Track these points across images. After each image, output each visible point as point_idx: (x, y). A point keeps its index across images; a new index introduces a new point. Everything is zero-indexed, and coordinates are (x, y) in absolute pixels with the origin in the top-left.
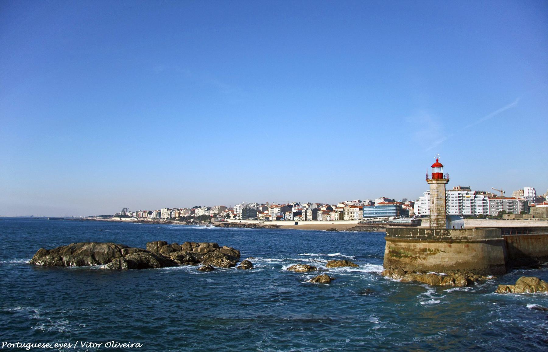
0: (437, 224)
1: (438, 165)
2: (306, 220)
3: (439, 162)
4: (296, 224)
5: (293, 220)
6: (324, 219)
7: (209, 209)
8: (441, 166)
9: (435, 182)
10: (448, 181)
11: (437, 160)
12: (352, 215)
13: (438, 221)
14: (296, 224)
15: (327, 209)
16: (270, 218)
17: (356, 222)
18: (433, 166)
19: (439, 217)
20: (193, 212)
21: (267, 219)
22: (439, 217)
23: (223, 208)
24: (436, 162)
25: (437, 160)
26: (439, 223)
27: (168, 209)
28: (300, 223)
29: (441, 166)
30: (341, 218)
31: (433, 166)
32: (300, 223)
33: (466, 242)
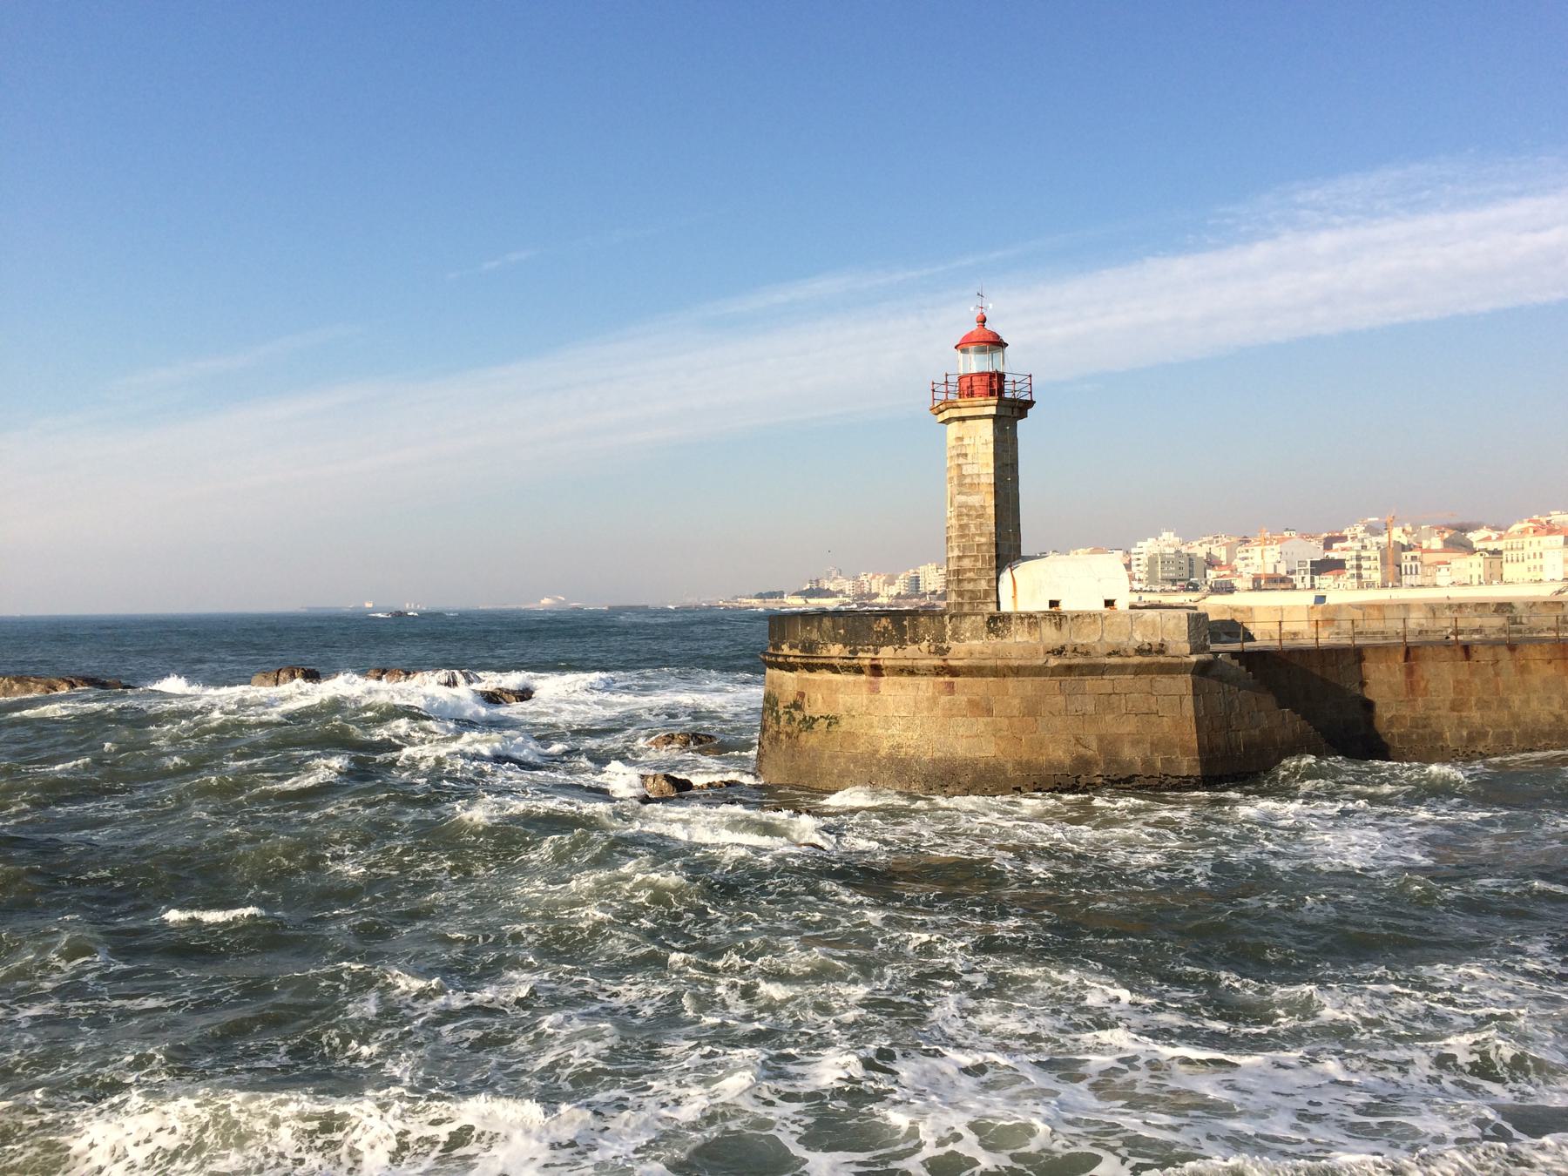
2: (1360, 586)
4: (1320, 599)
5: (1313, 587)
6: (1427, 581)
8: (997, 344)
10: (1030, 403)
12: (1538, 562)
13: (960, 581)
14: (1320, 599)
15: (1446, 542)
16: (1237, 583)
17: (1545, 592)
18: (962, 347)
19: (966, 563)
21: (1230, 589)
22: (966, 563)
24: (974, 326)
26: (970, 586)
28: (1332, 599)
30: (1494, 576)
32: (1332, 599)
33: (939, 671)
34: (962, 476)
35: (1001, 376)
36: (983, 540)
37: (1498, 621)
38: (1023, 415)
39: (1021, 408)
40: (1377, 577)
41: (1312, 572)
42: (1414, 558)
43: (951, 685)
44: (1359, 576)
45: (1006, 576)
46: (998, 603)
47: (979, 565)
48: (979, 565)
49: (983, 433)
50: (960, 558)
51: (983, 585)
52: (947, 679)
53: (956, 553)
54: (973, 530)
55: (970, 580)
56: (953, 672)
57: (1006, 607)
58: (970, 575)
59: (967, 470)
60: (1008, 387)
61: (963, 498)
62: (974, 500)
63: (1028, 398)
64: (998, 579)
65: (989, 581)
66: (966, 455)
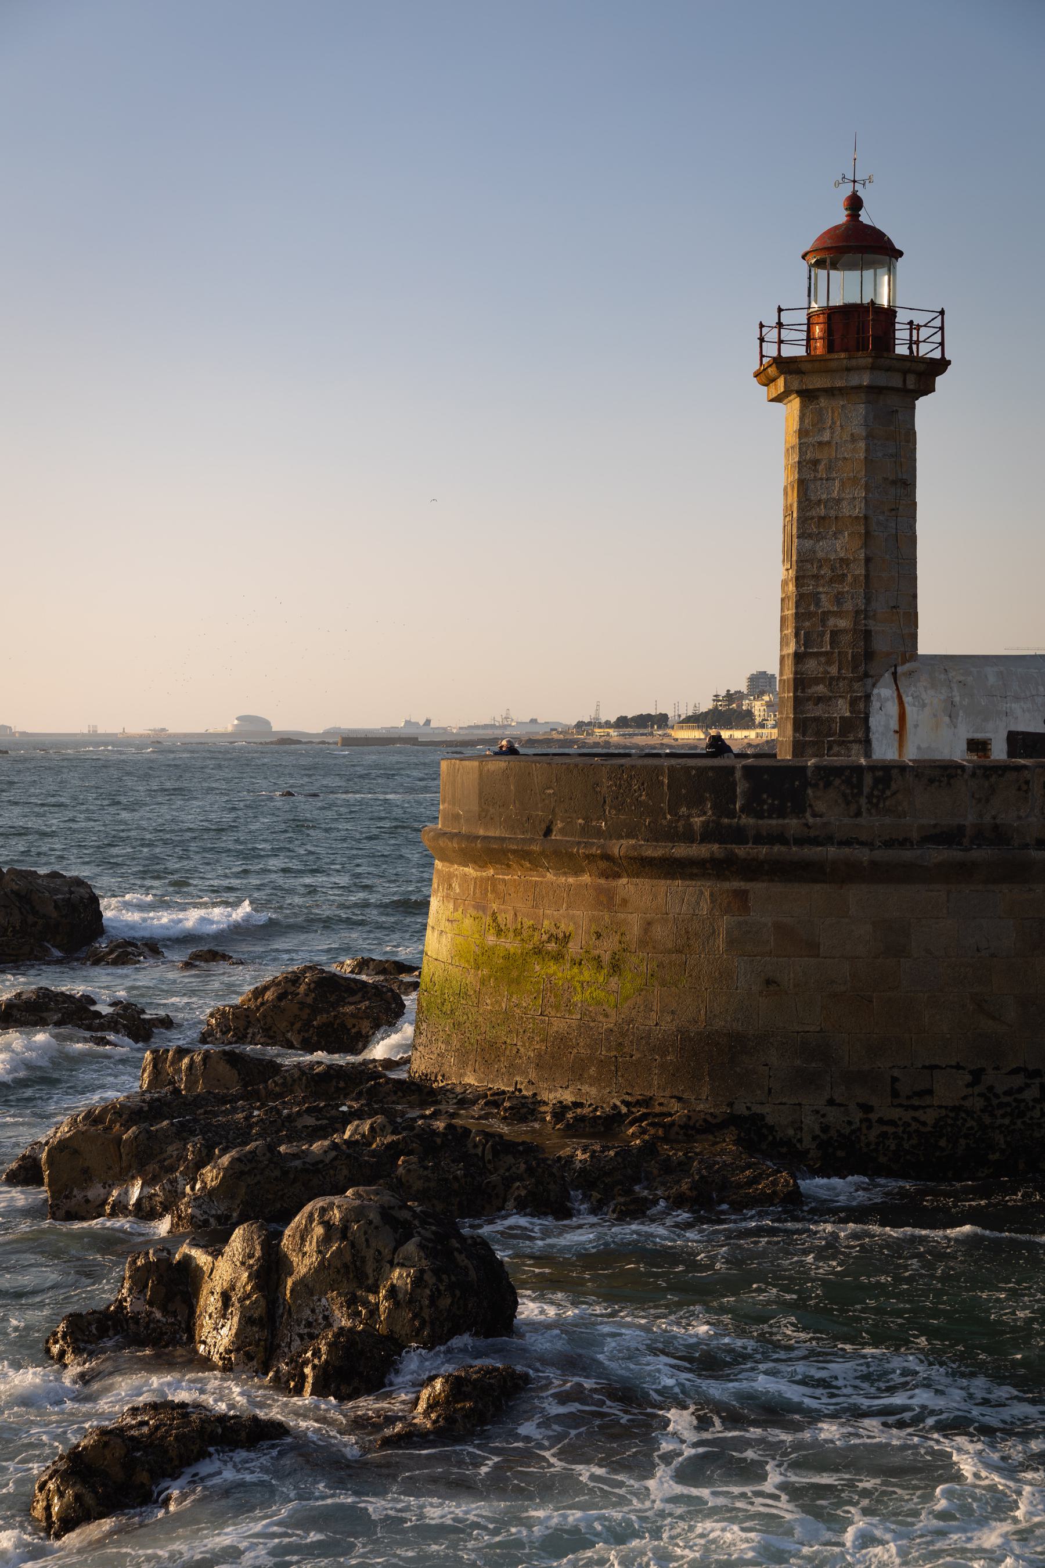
1: (858, 243)
3: (864, 218)
10: (941, 365)
11: (855, 204)
24: (840, 217)
25: (855, 204)
35: (889, 314)
36: (843, 623)
38: (929, 389)
39: (926, 373)
43: (742, 896)
45: (884, 692)
46: (867, 742)
47: (834, 670)
48: (834, 670)
51: (842, 708)
52: (737, 884)
54: (826, 604)
55: (819, 700)
56: (751, 870)
57: (884, 750)
58: (821, 689)
60: (902, 334)
61: (808, 544)
63: (937, 355)
64: (868, 697)
65: (853, 703)
66: (815, 463)
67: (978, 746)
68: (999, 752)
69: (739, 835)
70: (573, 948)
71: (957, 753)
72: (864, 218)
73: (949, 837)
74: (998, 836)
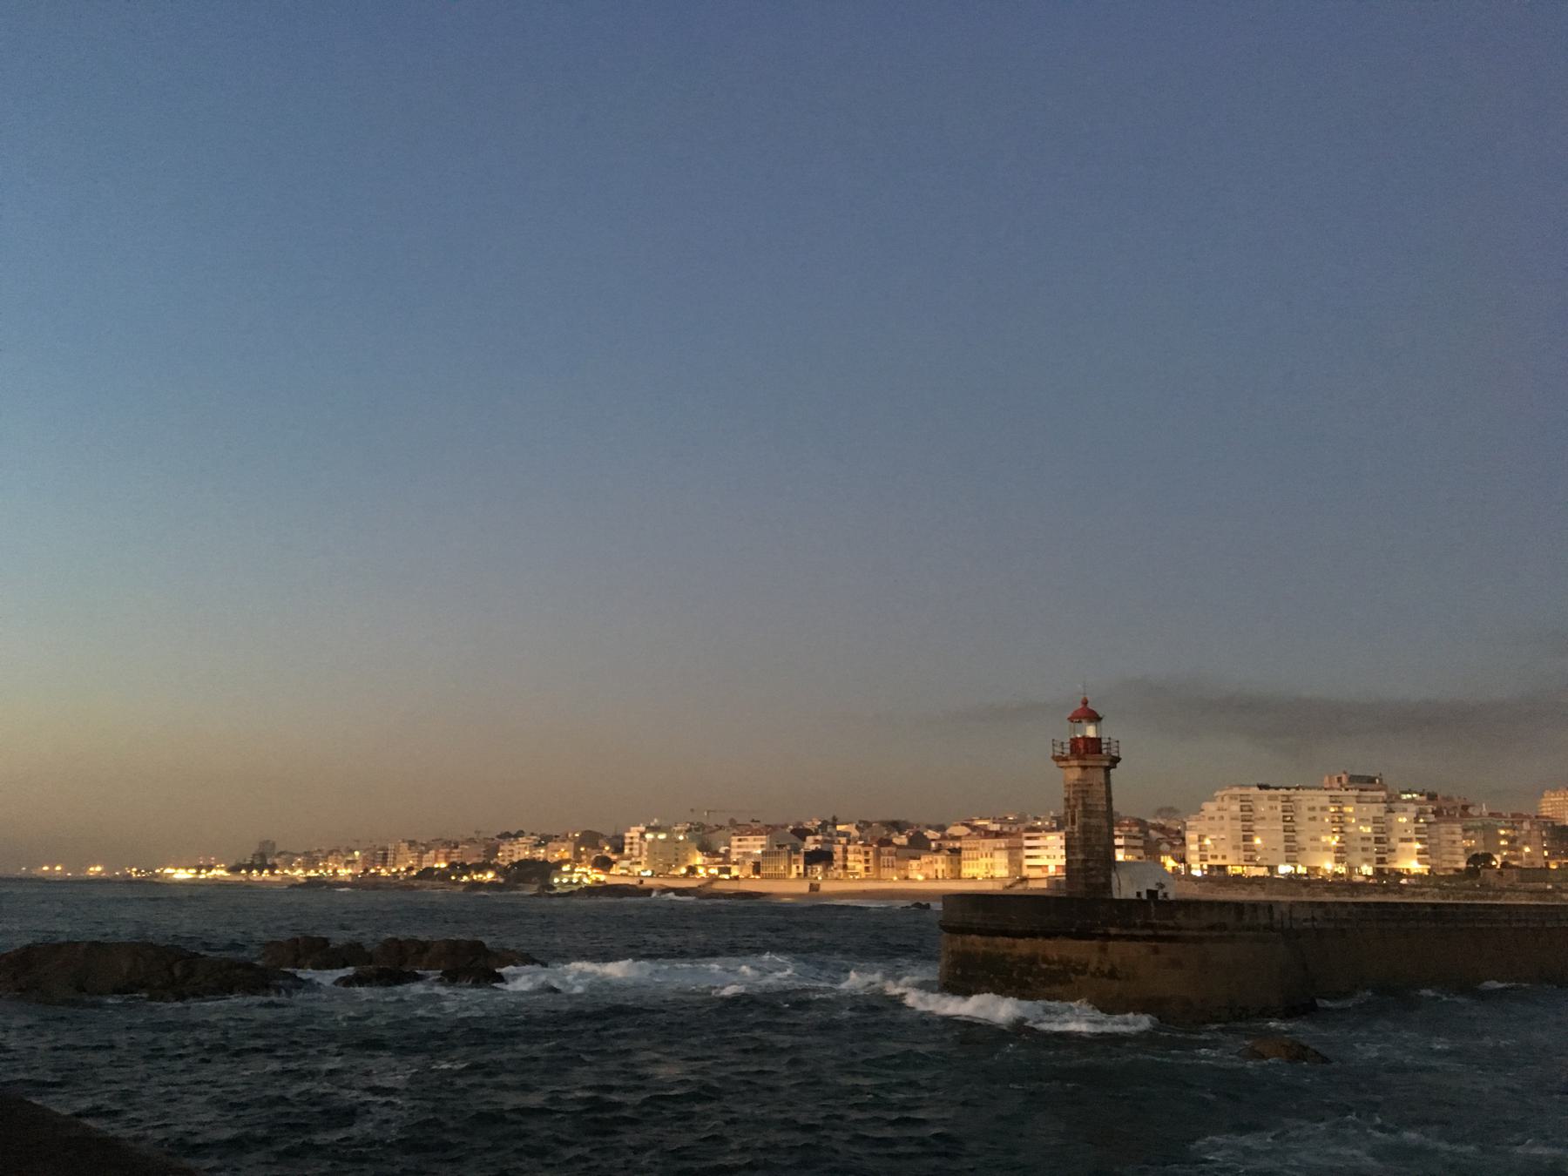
0: (1086, 885)
3: (1090, 706)
7: (544, 841)
9: (1075, 763)
10: (1118, 759)
11: (1085, 702)
12: (989, 860)
14: (814, 888)
15: (910, 840)
19: (1090, 864)
20: (493, 850)
22: (1090, 864)
23: (590, 839)
24: (1080, 706)
25: (1085, 702)
27: (412, 844)
28: (826, 887)
29: (1094, 718)
31: (1077, 718)
34: (1084, 805)
37: (1318, 913)
39: (1115, 761)
40: (860, 867)
41: (807, 863)
42: (890, 854)
44: (845, 867)
49: (1100, 776)
50: (1085, 861)
51: (1102, 880)
53: (1080, 857)
57: (1116, 896)
59: (1089, 801)
62: (1094, 821)
67: (1139, 894)
68: (1144, 896)
69: (1152, 926)
70: (1092, 968)
71: (1134, 897)
72: (1090, 706)
73: (1212, 928)
74: (1224, 927)
